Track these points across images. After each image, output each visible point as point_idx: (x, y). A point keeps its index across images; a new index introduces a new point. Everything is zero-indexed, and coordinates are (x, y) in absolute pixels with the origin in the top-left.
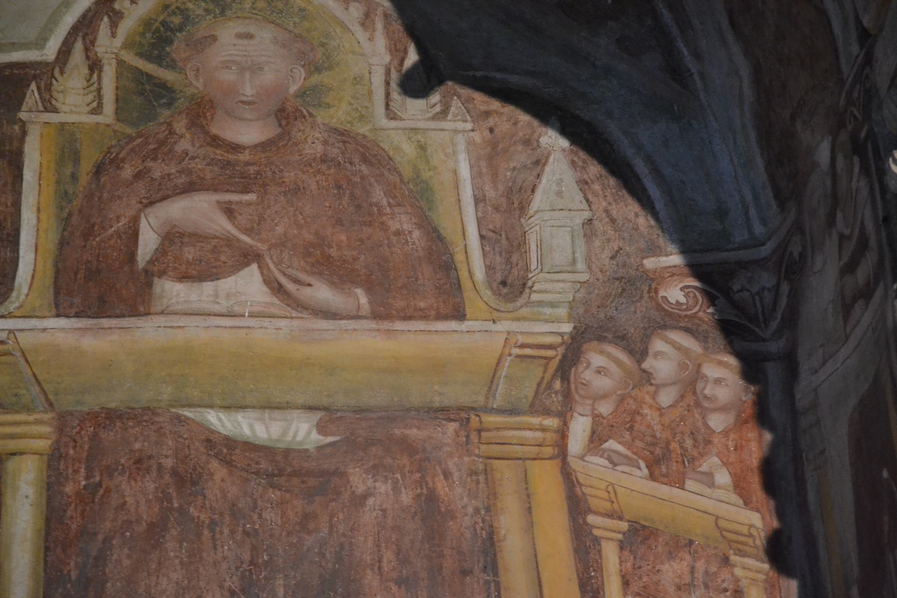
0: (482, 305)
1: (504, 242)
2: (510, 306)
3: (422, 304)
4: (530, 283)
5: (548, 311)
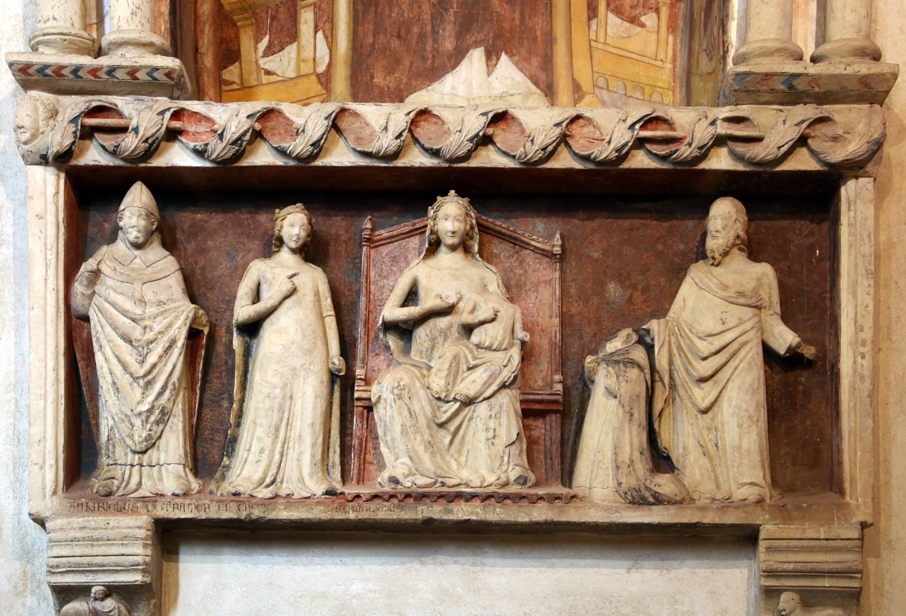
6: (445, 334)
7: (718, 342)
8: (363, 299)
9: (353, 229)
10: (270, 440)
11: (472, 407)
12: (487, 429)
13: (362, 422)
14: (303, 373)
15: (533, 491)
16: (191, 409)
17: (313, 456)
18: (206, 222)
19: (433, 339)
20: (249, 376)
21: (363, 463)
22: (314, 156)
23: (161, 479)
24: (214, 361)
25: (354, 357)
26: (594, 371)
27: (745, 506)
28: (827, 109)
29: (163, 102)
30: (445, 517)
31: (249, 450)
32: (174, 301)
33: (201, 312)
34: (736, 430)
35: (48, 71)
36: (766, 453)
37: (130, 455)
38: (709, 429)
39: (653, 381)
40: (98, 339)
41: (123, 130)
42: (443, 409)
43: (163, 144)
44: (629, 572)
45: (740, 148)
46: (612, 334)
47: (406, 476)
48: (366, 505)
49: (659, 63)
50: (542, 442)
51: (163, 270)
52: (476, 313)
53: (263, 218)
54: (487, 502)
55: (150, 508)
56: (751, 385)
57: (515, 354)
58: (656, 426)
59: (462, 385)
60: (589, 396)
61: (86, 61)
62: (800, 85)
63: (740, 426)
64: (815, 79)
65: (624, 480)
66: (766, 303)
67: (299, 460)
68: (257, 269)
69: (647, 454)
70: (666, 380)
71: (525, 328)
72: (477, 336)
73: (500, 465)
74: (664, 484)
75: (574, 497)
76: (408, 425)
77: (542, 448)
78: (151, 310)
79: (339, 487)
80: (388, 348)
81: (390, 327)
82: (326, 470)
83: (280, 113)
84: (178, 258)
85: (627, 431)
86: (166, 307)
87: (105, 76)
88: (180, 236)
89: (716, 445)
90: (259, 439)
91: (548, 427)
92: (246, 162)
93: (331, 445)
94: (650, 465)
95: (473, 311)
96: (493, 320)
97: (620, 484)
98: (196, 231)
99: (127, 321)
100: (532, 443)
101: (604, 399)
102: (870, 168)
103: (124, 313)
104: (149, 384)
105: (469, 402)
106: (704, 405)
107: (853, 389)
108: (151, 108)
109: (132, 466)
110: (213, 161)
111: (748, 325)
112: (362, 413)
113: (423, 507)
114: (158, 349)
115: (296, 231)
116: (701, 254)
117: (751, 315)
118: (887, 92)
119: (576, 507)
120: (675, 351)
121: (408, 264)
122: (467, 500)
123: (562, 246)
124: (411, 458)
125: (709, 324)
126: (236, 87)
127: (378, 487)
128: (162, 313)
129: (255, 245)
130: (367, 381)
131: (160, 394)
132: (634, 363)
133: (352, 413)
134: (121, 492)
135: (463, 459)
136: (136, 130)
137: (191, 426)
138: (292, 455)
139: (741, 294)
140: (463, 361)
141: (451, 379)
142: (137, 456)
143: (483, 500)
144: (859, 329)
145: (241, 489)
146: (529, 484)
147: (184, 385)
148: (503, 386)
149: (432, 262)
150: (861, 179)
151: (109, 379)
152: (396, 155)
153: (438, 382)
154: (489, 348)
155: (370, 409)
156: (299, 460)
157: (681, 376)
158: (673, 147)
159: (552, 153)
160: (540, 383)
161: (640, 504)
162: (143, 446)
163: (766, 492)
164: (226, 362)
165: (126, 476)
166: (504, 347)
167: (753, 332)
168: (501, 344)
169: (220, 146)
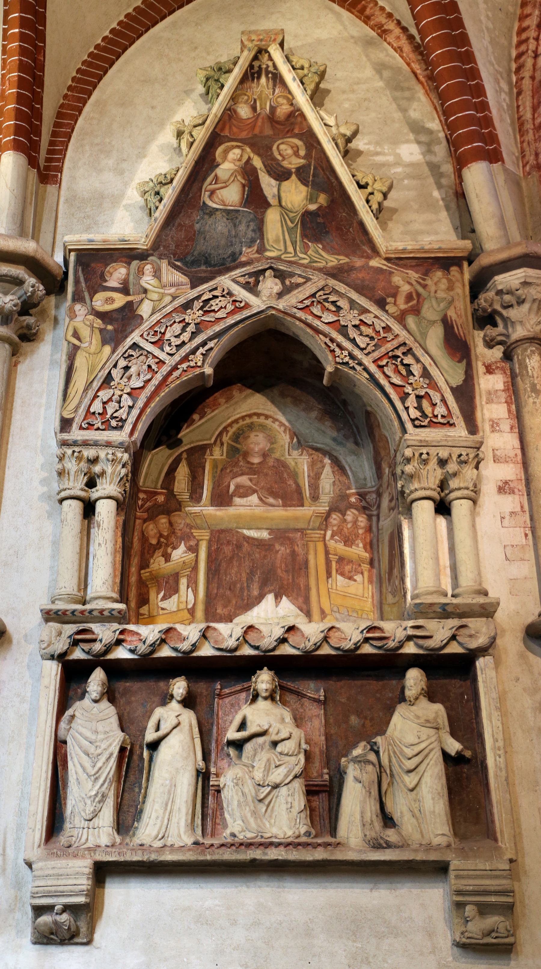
6: (262, 747)
7: (417, 749)
8: (215, 728)
9: (210, 689)
10: (162, 811)
11: (278, 789)
12: (287, 803)
13: (214, 799)
14: (182, 771)
15: (315, 841)
16: (118, 793)
17: (186, 820)
18: (132, 687)
19: (255, 750)
20: (151, 773)
21: (214, 824)
22: (192, 651)
23: (99, 837)
24: (132, 765)
25: (210, 761)
26: (346, 767)
27: (440, 849)
28: (464, 621)
29: (116, 626)
30: (263, 858)
31: (150, 818)
32: (113, 731)
33: (127, 737)
34: (431, 801)
35: (60, 613)
36: (449, 816)
37: (83, 821)
38: (415, 801)
39: (381, 772)
40: (71, 754)
41: (94, 640)
42: (261, 791)
43: (114, 647)
44: (371, 891)
45: (421, 642)
46: (354, 746)
47: (240, 832)
48: (217, 851)
49: (365, 599)
50: (317, 810)
51: (108, 714)
52: (279, 735)
53: (162, 684)
54: (288, 848)
55: (92, 854)
56: (438, 774)
57: (302, 757)
58: (384, 799)
59: (272, 776)
60: (343, 782)
61: (79, 607)
62: (449, 609)
63: (433, 799)
64: (457, 606)
65: (368, 833)
66: (441, 726)
67: (178, 823)
68: (159, 712)
69: (380, 817)
70: (388, 772)
71: (306, 743)
72: (279, 748)
73: (295, 824)
74: (391, 835)
75: (338, 844)
76: (242, 800)
77: (317, 813)
78: (101, 736)
79: (201, 840)
80: (229, 755)
81: (231, 743)
82: (193, 830)
83: (175, 629)
84: (116, 706)
85: (368, 803)
86: (109, 735)
87: (87, 614)
88: (117, 695)
89: (420, 811)
90: (156, 811)
91: (321, 801)
92: (156, 655)
93: (196, 813)
94: (382, 824)
95: (277, 733)
96: (289, 738)
97: (365, 835)
98: (126, 692)
99: (88, 743)
100: (312, 810)
101: (353, 784)
102: (490, 651)
103: (86, 738)
104: (96, 779)
105: (276, 786)
106: (411, 786)
107: (496, 776)
108: (109, 629)
109: (84, 828)
110: (139, 655)
111: (433, 739)
112: (214, 794)
113: (251, 852)
114: (103, 759)
115: (181, 691)
116: (402, 699)
117: (434, 733)
118: (495, 612)
119: (340, 850)
120: (392, 754)
121: (240, 708)
122: (276, 847)
123: (325, 696)
124: (243, 821)
125: (411, 738)
126: (146, 616)
127: (224, 839)
128: (106, 738)
129: (157, 699)
130: (217, 775)
131: (102, 785)
132: (369, 762)
133: (208, 794)
134: (76, 845)
135: (273, 821)
136: (101, 641)
137: (117, 803)
138: (174, 820)
139: (427, 721)
140: (272, 762)
141: (266, 773)
142: (86, 822)
143: (286, 847)
144: (496, 740)
145: (144, 842)
146: (312, 836)
147: (115, 779)
148: (296, 777)
149: (254, 706)
150: (486, 657)
151: (75, 777)
152: (236, 649)
153: (258, 775)
154: (287, 755)
155: (219, 791)
156: (178, 823)
157: (396, 769)
158: (384, 642)
159: (319, 646)
160: (315, 774)
161: (378, 848)
162: (90, 817)
163: (452, 839)
164: (138, 765)
165: (80, 835)
166: (295, 753)
167: (436, 742)
168: (293, 752)
169: (144, 647)
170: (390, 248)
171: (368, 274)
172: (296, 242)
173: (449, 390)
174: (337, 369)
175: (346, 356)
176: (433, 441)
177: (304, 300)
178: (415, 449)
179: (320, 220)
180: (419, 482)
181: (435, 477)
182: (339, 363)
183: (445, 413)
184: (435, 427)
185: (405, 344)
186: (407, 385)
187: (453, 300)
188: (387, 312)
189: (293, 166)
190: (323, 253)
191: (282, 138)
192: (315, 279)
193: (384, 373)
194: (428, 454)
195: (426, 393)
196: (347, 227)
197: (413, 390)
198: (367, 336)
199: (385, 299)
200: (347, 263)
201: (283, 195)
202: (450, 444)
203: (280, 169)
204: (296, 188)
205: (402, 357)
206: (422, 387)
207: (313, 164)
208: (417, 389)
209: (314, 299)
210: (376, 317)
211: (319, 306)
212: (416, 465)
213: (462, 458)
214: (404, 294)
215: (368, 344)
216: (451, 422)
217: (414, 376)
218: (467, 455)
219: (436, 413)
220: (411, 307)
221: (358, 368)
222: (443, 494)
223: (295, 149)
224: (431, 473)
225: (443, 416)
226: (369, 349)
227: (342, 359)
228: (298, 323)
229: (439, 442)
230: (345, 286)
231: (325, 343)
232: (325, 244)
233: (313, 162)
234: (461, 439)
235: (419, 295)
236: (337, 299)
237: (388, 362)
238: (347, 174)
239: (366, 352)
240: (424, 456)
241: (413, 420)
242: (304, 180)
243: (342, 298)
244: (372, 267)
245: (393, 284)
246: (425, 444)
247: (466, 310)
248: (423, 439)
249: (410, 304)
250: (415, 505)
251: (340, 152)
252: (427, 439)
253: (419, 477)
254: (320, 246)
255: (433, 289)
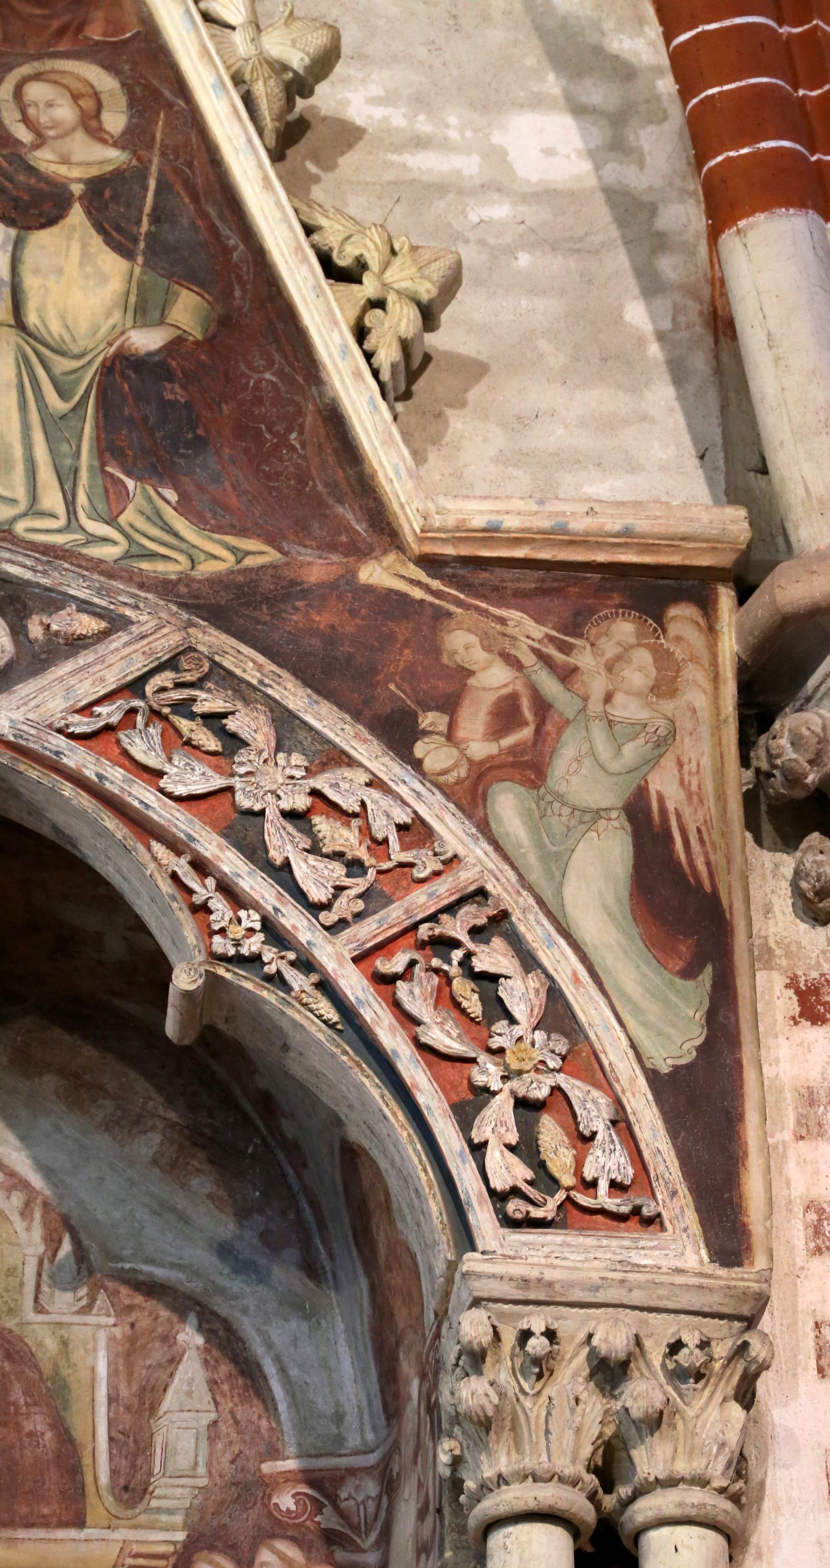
0: (101, 1509)
1: (131, 1443)
2: (130, 1513)
3: (46, 1511)
4: (151, 1488)
5: (164, 1518)
170: (437, 521)
171: (353, 613)
172: (76, 471)
173: (642, 1081)
174: (213, 982)
175: (251, 931)
176: (572, 1285)
177: (98, 702)
178: (501, 1315)
179: (174, 392)
180: (519, 1449)
181: (578, 1431)
182: (224, 959)
183: (627, 1174)
184: (583, 1229)
185: (481, 894)
186: (483, 1058)
187: (673, 733)
188: (417, 765)
189: (76, 173)
190: (181, 525)
191: (39, 57)
192: (144, 620)
193: (396, 1006)
194: (550, 1335)
195: (556, 1089)
196: (280, 428)
197: (505, 1078)
198: (337, 856)
199: (414, 717)
200: (274, 566)
201: (30, 282)
202: (638, 1297)
203: (21, 177)
204: (86, 257)
205: (471, 945)
206: (541, 1067)
207: (154, 169)
208: (520, 1073)
209: (137, 703)
210: (375, 783)
211: (155, 731)
212: (504, 1377)
213: (683, 1356)
214: (490, 699)
215: (339, 889)
216: (645, 1211)
217: (513, 1021)
218: (704, 1345)
219: (589, 1173)
220: (513, 751)
221: (297, 980)
222: (609, 1501)
223: (88, 104)
224: (561, 1413)
225: (615, 1186)
226: (344, 907)
227: (237, 944)
228: (68, 790)
229: (596, 1289)
230: (261, 659)
231: (174, 876)
232: (191, 489)
233: (156, 160)
234: (679, 1280)
235: (542, 707)
236: (229, 707)
237: (412, 964)
238: (285, 219)
239: (329, 917)
240: (537, 1345)
241: (499, 1198)
242: (118, 229)
243: (246, 702)
244: (369, 589)
245: (445, 659)
246: (542, 1297)
247: (719, 771)
248: (534, 1274)
249: (508, 741)
250: (496, 1539)
251: (260, 132)
252: (549, 1275)
253: (514, 1428)
254: (171, 495)
255: (598, 685)
